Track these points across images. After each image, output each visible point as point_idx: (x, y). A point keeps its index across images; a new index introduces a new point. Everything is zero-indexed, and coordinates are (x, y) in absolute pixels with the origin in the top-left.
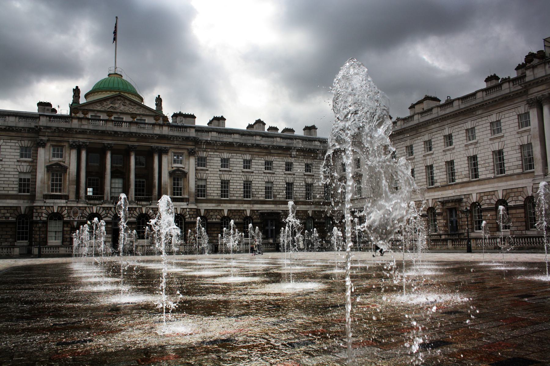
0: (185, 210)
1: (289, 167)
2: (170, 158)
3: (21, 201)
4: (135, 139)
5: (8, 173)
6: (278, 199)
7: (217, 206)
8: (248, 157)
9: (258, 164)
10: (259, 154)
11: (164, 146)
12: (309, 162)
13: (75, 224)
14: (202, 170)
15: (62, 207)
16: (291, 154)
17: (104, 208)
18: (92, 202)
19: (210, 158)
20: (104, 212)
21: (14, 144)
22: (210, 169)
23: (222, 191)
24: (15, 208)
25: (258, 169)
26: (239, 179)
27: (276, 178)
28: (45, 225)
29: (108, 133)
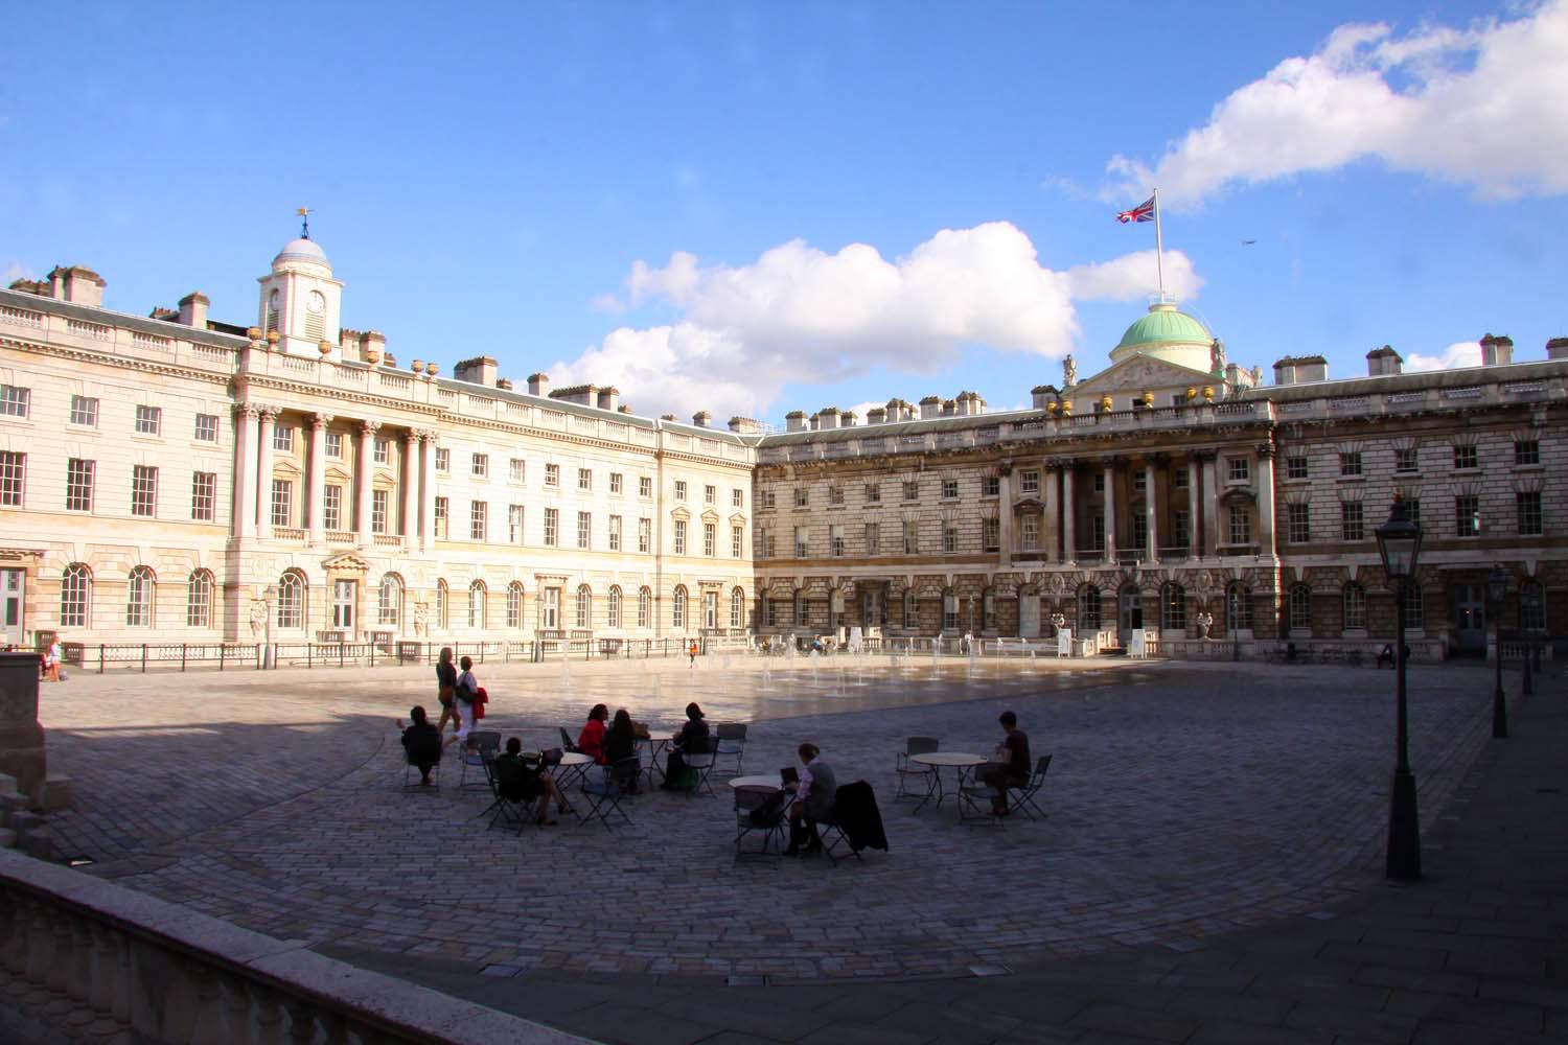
0: (1251, 571)
1: (1527, 452)
3: (988, 566)
4: (1152, 441)
6: (1490, 536)
7: (1334, 559)
8: (1405, 443)
9: (1436, 456)
10: (1435, 433)
11: (1204, 446)
13: (1057, 601)
14: (1297, 484)
15: (1037, 574)
16: (1531, 420)
17: (1101, 572)
18: (1086, 562)
19: (1315, 458)
20: (1103, 580)
22: (1314, 482)
23: (1346, 527)
24: (978, 577)
25: (1436, 468)
27: (1487, 484)
28: (1014, 604)
29: (1101, 438)
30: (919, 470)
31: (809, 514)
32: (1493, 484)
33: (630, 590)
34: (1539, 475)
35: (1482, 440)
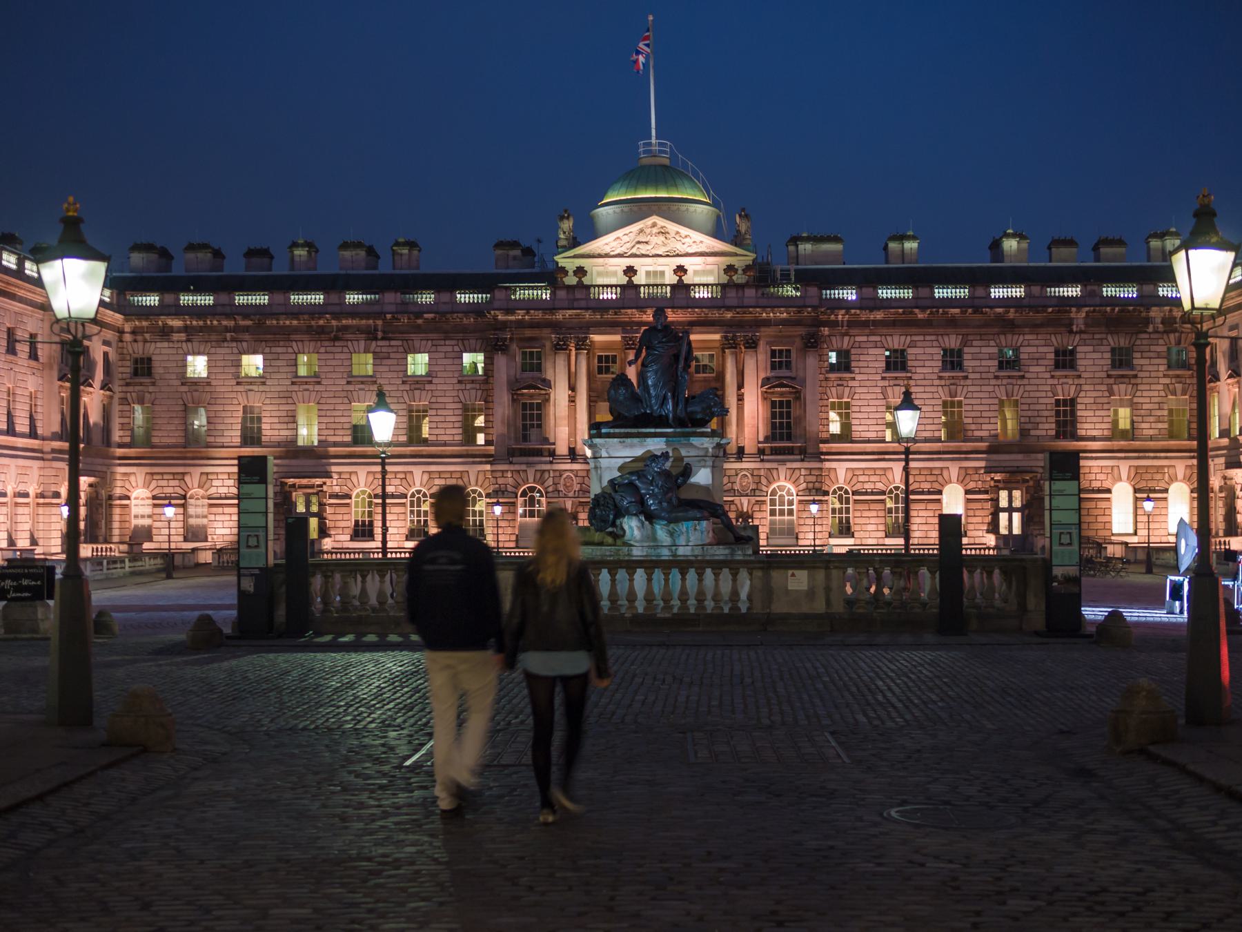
0: (797, 472)
2: (761, 357)
5: (442, 406)
8: (953, 342)
12: (1123, 342)
15: (544, 471)
19: (859, 351)
21: (450, 349)
25: (981, 369)
26: (930, 396)
27: (1028, 388)
30: (376, 339)
31: (208, 388)
32: (1035, 388)
34: (1076, 381)
35: (1026, 343)
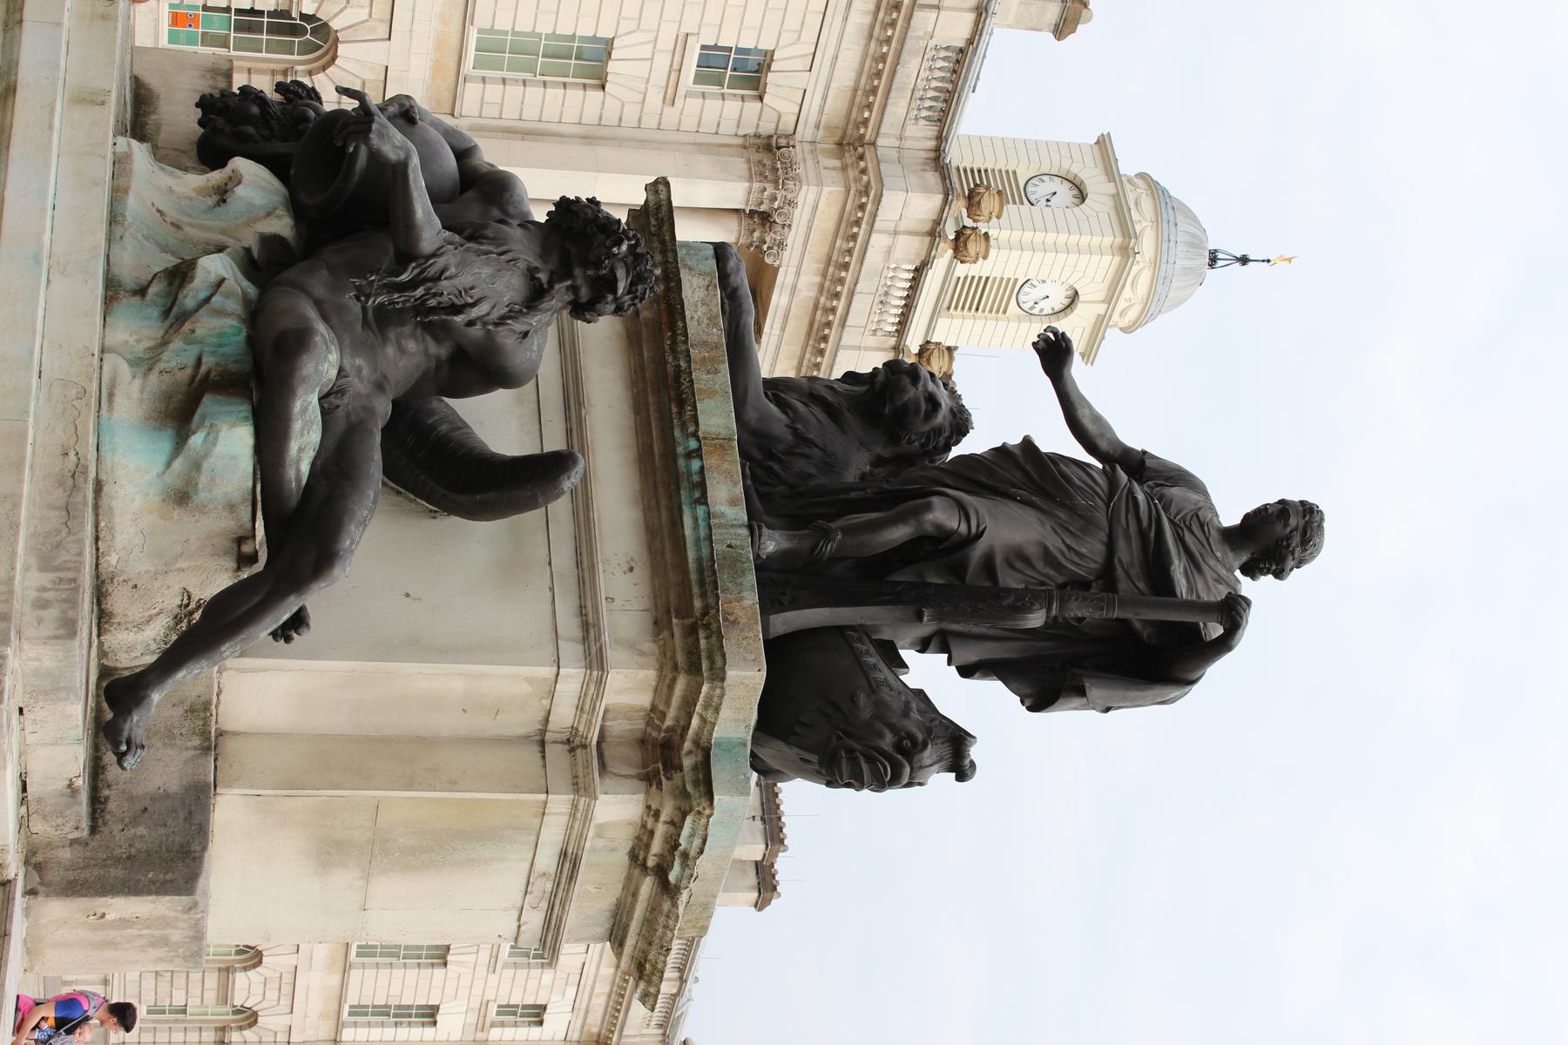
33: (247, 989)
